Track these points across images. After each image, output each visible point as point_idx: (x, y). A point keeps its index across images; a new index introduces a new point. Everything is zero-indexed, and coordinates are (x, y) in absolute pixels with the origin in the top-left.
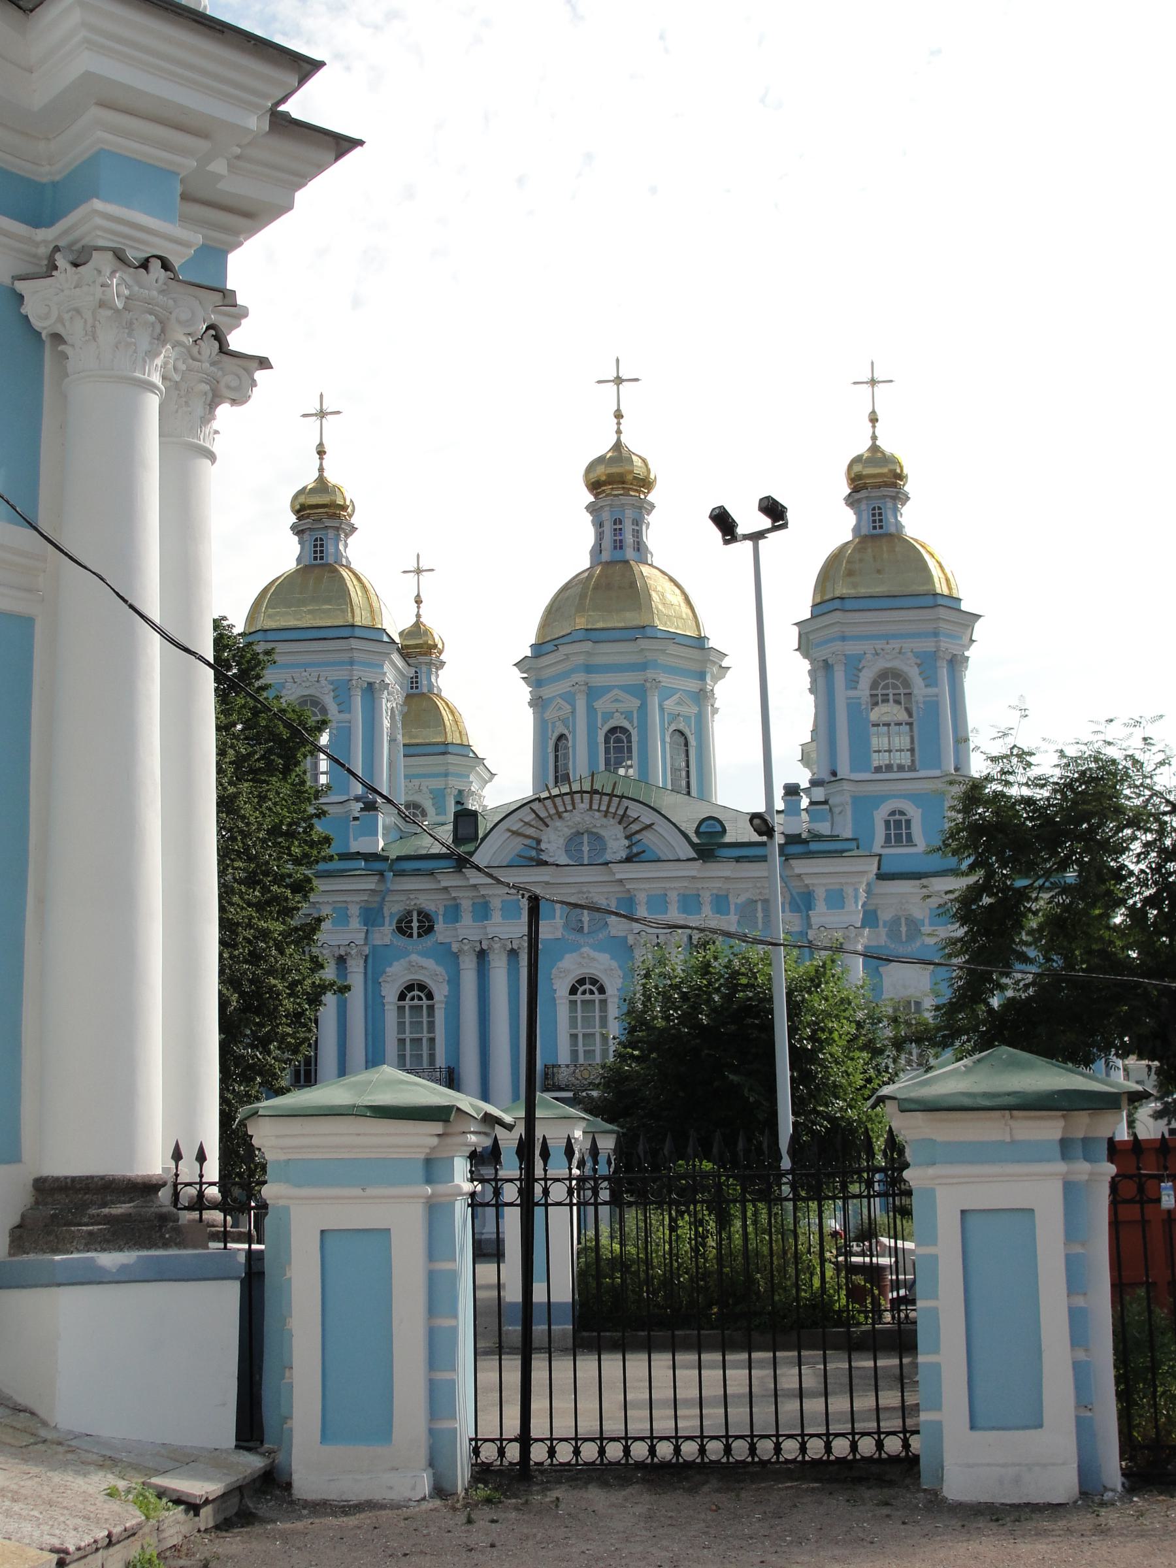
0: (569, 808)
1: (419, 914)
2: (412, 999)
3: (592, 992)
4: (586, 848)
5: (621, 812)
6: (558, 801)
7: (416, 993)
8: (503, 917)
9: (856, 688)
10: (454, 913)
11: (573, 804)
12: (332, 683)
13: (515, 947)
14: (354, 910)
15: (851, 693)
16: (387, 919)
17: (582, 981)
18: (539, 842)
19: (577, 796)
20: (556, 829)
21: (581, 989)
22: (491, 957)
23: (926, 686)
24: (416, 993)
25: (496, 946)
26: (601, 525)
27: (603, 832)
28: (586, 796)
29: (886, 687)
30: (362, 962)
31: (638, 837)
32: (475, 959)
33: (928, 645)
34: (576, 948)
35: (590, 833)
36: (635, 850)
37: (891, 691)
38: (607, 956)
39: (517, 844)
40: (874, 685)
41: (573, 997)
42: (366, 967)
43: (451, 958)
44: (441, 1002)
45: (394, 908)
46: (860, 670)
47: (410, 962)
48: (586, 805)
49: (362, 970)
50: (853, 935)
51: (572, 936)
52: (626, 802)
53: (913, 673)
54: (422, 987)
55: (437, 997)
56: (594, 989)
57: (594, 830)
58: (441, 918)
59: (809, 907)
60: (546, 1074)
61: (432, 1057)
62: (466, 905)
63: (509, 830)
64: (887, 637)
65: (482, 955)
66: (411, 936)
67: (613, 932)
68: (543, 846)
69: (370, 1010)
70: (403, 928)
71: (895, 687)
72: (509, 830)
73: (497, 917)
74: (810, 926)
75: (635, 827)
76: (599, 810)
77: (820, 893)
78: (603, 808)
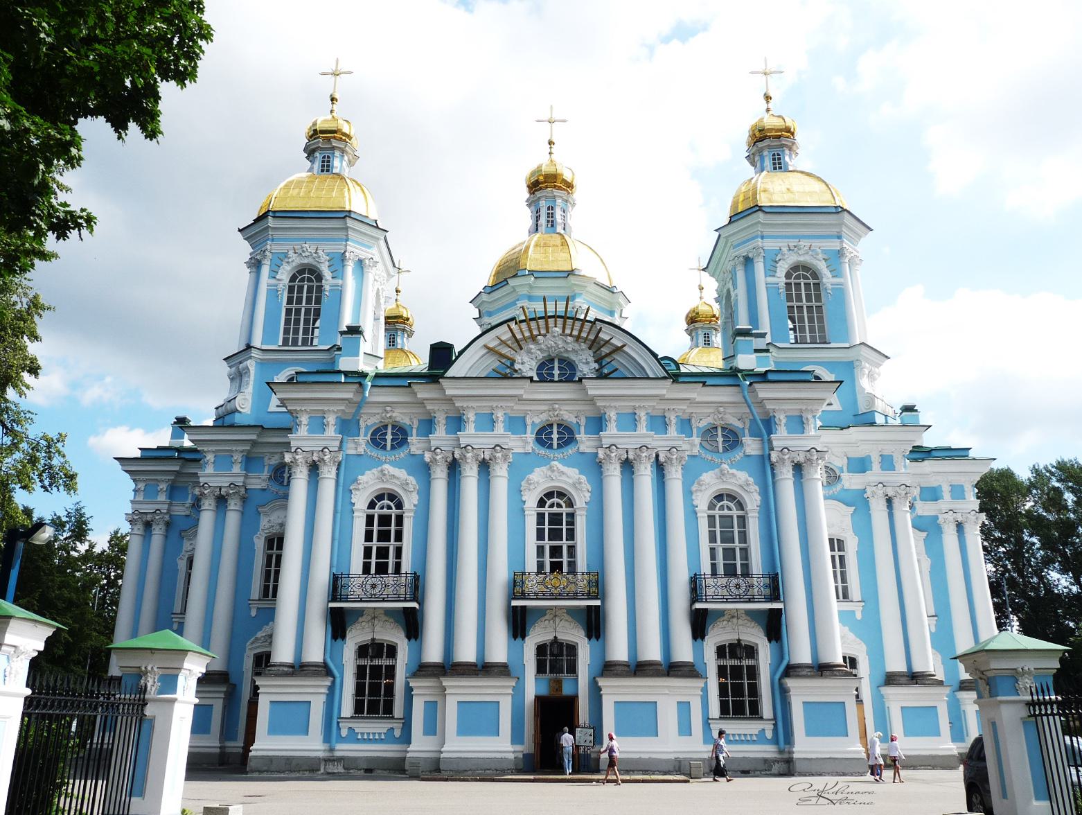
0: (543, 332)
1: (394, 427)
2: (382, 508)
3: (559, 506)
5: (592, 337)
6: (533, 324)
7: (386, 502)
8: (476, 429)
9: (774, 276)
10: (428, 425)
12: (328, 255)
13: (487, 457)
14: (331, 419)
15: (770, 279)
16: (362, 431)
17: (549, 495)
18: (513, 362)
19: (551, 321)
20: (529, 352)
21: (549, 503)
22: (462, 467)
23: (833, 277)
24: (386, 502)
25: (469, 455)
26: (538, 211)
27: (573, 357)
28: (560, 321)
29: (798, 277)
31: (608, 360)
32: (446, 471)
33: (834, 245)
34: (545, 461)
35: (561, 361)
36: (606, 371)
37: (802, 281)
38: (577, 471)
39: (493, 363)
40: (788, 276)
42: (338, 475)
43: (424, 470)
44: (409, 510)
45: (369, 421)
46: (776, 262)
47: (382, 471)
48: (558, 330)
49: (333, 475)
50: (815, 458)
51: (542, 451)
52: (599, 325)
53: (822, 267)
54: (392, 497)
55: (407, 506)
56: (561, 502)
57: (566, 355)
58: (414, 431)
59: (770, 432)
60: (515, 581)
61: (398, 567)
62: (441, 419)
63: (486, 346)
64: (800, 237)
65: (454, 467)
66: (384, 448)
67: (583, 448)
68: (517, 367)
69: (339, 515)
70: (377, 440)
71: (805, 277)
72: (486, 346)
73: (470, 428)
74: (772, 449)
75: (605, 350)
76: (571, 335)
77: (781, 418)
78: (575, 333)
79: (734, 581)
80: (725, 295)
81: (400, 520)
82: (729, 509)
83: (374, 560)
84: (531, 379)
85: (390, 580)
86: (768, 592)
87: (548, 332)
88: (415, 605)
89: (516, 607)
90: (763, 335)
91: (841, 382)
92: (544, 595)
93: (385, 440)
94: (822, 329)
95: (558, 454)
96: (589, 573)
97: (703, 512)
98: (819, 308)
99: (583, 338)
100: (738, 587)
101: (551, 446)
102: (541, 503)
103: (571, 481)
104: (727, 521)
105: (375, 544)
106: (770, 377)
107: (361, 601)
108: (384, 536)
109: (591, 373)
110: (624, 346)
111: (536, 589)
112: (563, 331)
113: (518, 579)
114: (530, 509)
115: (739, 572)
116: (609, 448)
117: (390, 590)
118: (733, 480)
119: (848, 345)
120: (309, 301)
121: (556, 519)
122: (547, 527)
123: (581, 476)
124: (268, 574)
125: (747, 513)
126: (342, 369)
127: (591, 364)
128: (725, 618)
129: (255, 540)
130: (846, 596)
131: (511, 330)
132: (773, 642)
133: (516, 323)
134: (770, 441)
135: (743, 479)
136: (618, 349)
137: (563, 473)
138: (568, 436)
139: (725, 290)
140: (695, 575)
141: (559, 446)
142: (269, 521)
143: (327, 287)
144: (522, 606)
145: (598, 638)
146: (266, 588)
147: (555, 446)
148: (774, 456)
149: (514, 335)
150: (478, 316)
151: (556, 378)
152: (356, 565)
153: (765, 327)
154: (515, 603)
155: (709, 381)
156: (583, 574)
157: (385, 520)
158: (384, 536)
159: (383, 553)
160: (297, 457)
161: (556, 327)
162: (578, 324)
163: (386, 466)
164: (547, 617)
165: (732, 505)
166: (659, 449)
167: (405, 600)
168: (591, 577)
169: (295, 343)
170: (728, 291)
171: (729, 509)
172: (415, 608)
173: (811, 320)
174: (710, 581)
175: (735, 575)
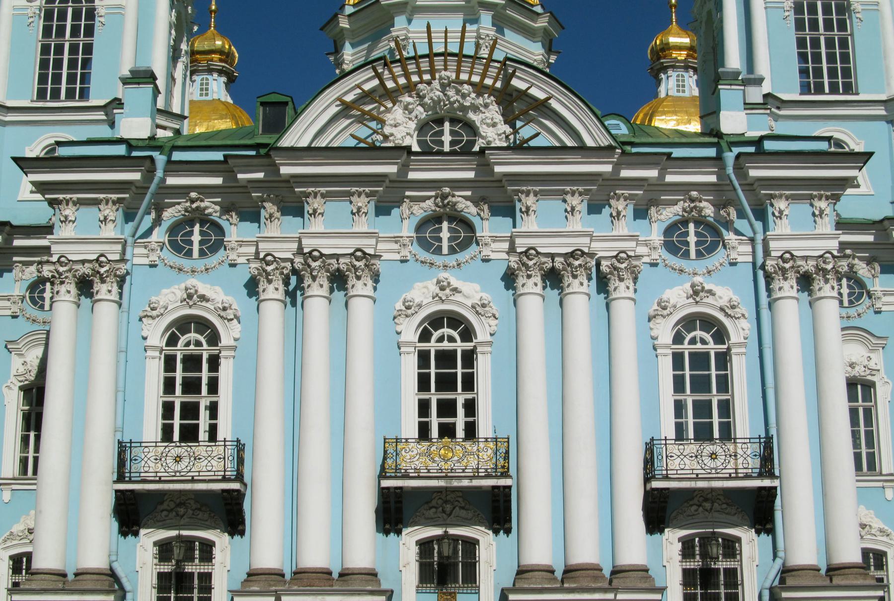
0: (427, 77)
3: (451, 339)
4: (447, 138)
7: (193, 336)
11: (432, 72)
18: (382, 122)
19: (439, 62)
21: (436, 335)
27: (471, 115)
30: (115, 289)
38: (477, 287)
41: (424, 346)
42: (121, 294)
49: (114, 296)
54: (203, 325)
56: (455, 334)
60: (385, 452)
66: (189, 254)
74: (767, 253)
79: (709, 448)
80: (704, 20)
81: (214, 364)
82: (703, 342)
83: (177, 422)
84: (408, 149)
85: (201, 449)
86: (757, 463)
87: (434, 78)
88: (236, 486)
89: (388, 488)
90: (759, 81)
91: (870, 154)
92: (429, 472)
93: (191, 243)
94: (847, 73)
95: (451, 260)
96: (496, 440)
97: (666, 347)
98: (844, 43)
99: (487, 87)
100: (713, 456)
101: (438, 251)
102: (425, 336)
103: (469, 303)
104: (700, 360)
105: (178, 398)
106: (769, 145)
107: (160, 481)
108: (192, 386)
109: (500, 140)
110: (549, 98)
111: (418, 463)
112: (458, 76)
113: (391, 450)
114: (408, 344)
115: (716, 434)
116: (526, 252)
117: (202, 465)
118: (710, 300)
119: (884, 97)
120: (75, 31)
121: (446, 358)
122: (433, 371)
123: (485, 295)
124: (25, 440)
125: (729, 349)
126: (125, 137)
127: (499, 126)
128: (695, 501)
129: (5, 391)
130: (872, 466)
131: (378, 76)
132: (763, 536)
133: (386, 64)
134: (765, 242)
135: (726, 299)
136: (543, 107)
137: (455, 290)
138: (466, 234)
139: (704, 14)
140: (652, 439)
141: (452, 251)
142: (25, 363)
143: (100, 11)
144: (396, 488)
145: (508, 531)
146: (24, 462)
147: (445, 250)
148: (769, 263)
149: (382, 83)
150: (333, 50)
151: (447, 148)
152: (151, 429)
153: (763, 67)
154: (386, 483)
155: (677, 153)
156: (486, 439)
157: (192, 362)
158: (192, 386)
159: (190, 411)
160: (61, 269)
161: (446, 69)
162: (479, 69)
163: (192, 281)
164: (434, 503)
165: (708, 337)
166: (600, 254)
167: (225, 479)
168: (499, 444)
169: (56, 95)
170: (709, 13)
171: (703, 342)
172: (238, 491)
173: (831, 58)
174: (674, 449)
175: (710, 439)
